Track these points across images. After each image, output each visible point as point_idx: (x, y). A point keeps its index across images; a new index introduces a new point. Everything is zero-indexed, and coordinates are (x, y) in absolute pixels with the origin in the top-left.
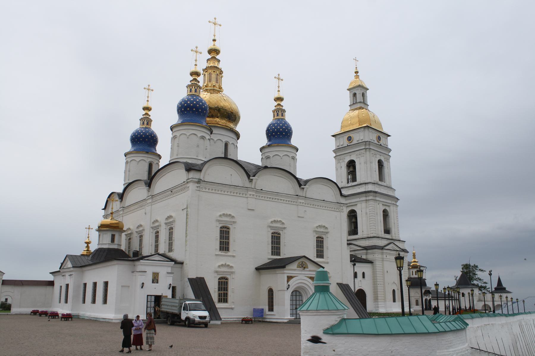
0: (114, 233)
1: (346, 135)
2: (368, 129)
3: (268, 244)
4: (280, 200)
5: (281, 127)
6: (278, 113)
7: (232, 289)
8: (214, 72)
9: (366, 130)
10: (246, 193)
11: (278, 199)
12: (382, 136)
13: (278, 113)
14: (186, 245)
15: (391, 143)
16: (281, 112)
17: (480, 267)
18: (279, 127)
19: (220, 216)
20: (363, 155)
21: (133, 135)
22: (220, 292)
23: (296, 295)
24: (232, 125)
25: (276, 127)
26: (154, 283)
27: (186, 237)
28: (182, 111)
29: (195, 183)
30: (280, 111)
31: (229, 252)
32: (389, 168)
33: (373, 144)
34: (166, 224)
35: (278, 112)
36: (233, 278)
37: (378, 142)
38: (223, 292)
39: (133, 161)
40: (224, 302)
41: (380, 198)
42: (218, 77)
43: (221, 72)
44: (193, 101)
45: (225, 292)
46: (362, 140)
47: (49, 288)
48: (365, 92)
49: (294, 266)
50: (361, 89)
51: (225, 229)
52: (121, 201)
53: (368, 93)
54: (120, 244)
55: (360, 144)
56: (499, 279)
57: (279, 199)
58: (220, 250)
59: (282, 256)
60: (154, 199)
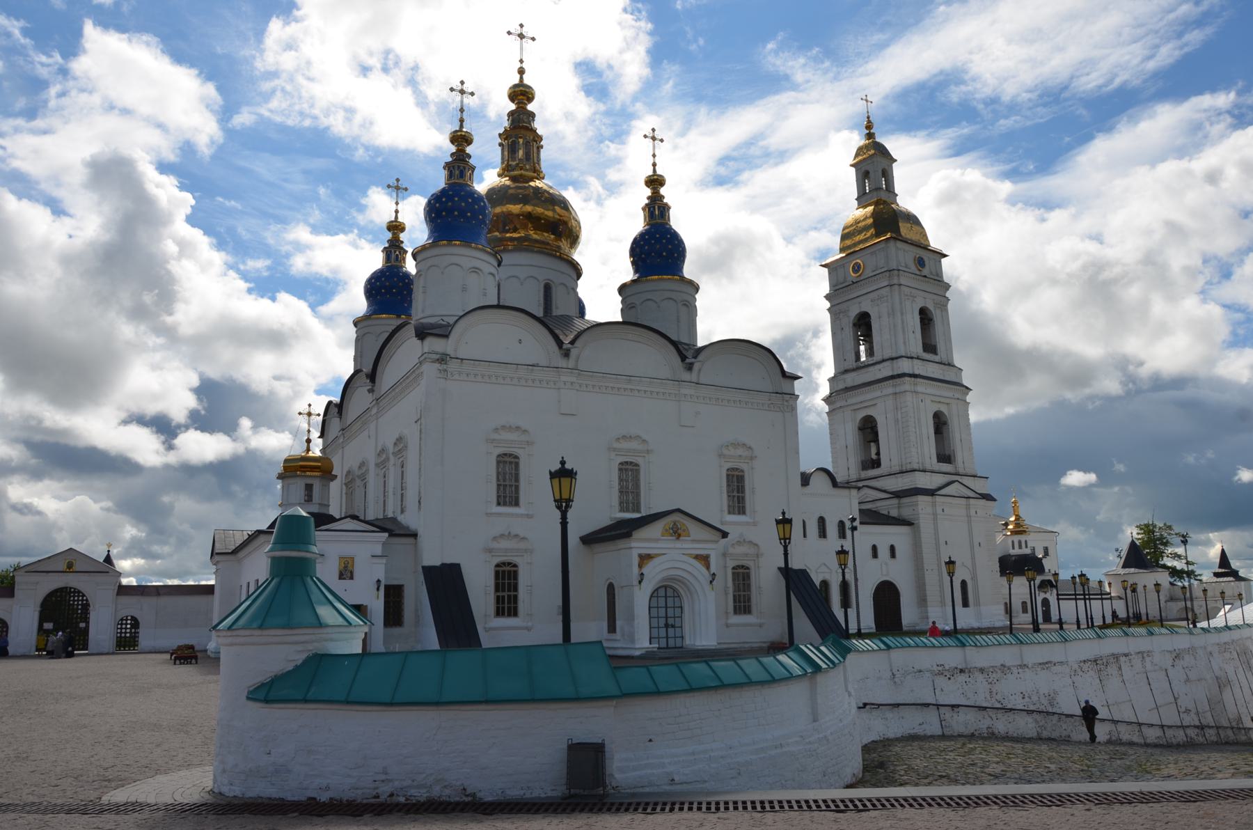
22: (500, 594)
38: (506, 594)
40: (509, 615)
45: (512, 593)
58: (499, 504)
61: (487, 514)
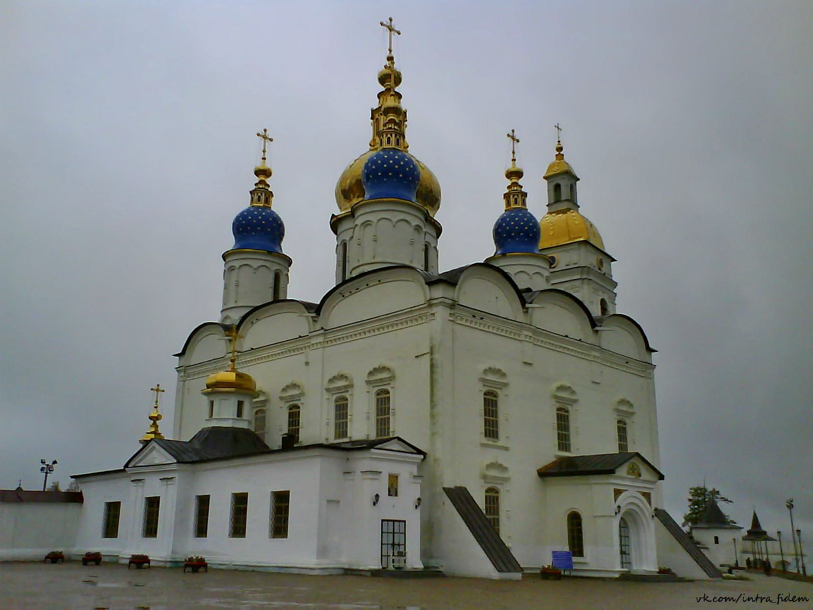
7: (508, 511)
12: (605, 260)
13: (516, 199)
15: (616, 271)
17: (723, 494)
29: (446, 307)
36: (508, 491)
37: (600, 269)
56: (755, 514)
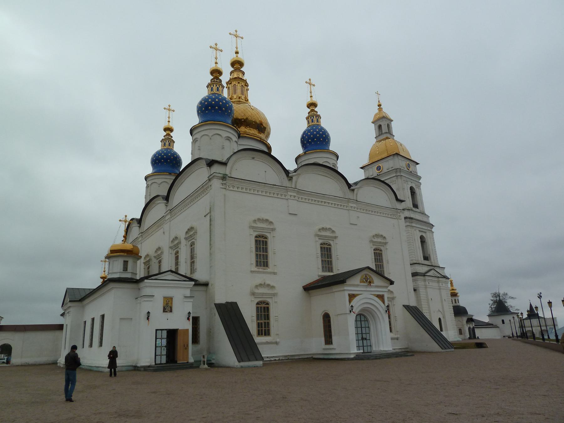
0: (126, 259)
1: (374, 165)
2: (398, 157)
3: (317, 257)
4: (327, 203)
5: (318, 133)
6: (312, 119)
8: (239, 83)
9: (396, 157)
10: (286, 194)
11: (325, 202)
13: (312, 119)
14: (211, 260)
15: (420, 170)
16: (316, 118)
18: (315, 133)
19: (255, 221)
20: (395, 182)
21: (153, 157)
23: (361, 321)
24: (262, 136)
25: (312, 133)
26: (166, 312)
27: (210, 249)
28: (202, 111)
29: (219, 179)
30: (315, 117)
31: (269, 268)
32: (421, 195)
33: (404, 171)
34: (186, 239)
35: (312, 118)
37: (408, 170)
39: (153, 184)
41: (416, 224)
42: (243, 89)
43: (247, 85)
44: (215, 99)
46: (393, 167)
47: (57, 333)
48: (390, 123)
49: (356, 280)
50: (386, 120)
51: (261, 239)
52: (140, 227)
53: (393, 124)
54: (135, 272)
55: (390, 172)
57: (326, 202)
58: (257, 265)
59: (335, 272)
60: (173, 213)
61: (251, 271)
